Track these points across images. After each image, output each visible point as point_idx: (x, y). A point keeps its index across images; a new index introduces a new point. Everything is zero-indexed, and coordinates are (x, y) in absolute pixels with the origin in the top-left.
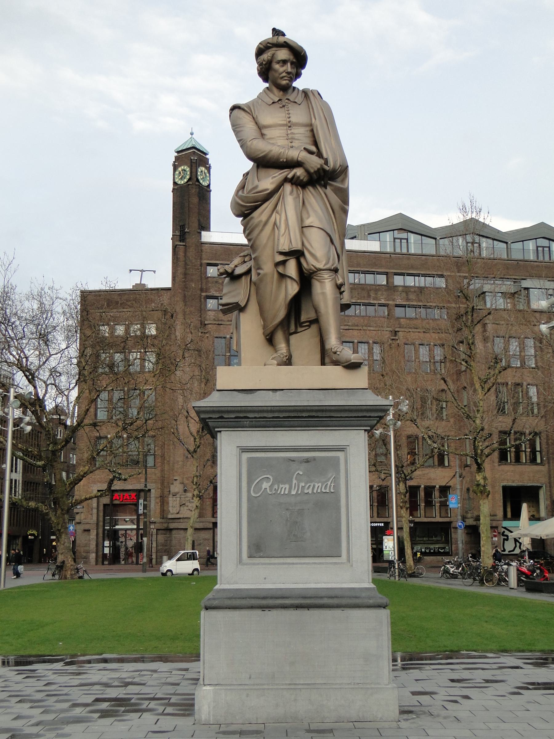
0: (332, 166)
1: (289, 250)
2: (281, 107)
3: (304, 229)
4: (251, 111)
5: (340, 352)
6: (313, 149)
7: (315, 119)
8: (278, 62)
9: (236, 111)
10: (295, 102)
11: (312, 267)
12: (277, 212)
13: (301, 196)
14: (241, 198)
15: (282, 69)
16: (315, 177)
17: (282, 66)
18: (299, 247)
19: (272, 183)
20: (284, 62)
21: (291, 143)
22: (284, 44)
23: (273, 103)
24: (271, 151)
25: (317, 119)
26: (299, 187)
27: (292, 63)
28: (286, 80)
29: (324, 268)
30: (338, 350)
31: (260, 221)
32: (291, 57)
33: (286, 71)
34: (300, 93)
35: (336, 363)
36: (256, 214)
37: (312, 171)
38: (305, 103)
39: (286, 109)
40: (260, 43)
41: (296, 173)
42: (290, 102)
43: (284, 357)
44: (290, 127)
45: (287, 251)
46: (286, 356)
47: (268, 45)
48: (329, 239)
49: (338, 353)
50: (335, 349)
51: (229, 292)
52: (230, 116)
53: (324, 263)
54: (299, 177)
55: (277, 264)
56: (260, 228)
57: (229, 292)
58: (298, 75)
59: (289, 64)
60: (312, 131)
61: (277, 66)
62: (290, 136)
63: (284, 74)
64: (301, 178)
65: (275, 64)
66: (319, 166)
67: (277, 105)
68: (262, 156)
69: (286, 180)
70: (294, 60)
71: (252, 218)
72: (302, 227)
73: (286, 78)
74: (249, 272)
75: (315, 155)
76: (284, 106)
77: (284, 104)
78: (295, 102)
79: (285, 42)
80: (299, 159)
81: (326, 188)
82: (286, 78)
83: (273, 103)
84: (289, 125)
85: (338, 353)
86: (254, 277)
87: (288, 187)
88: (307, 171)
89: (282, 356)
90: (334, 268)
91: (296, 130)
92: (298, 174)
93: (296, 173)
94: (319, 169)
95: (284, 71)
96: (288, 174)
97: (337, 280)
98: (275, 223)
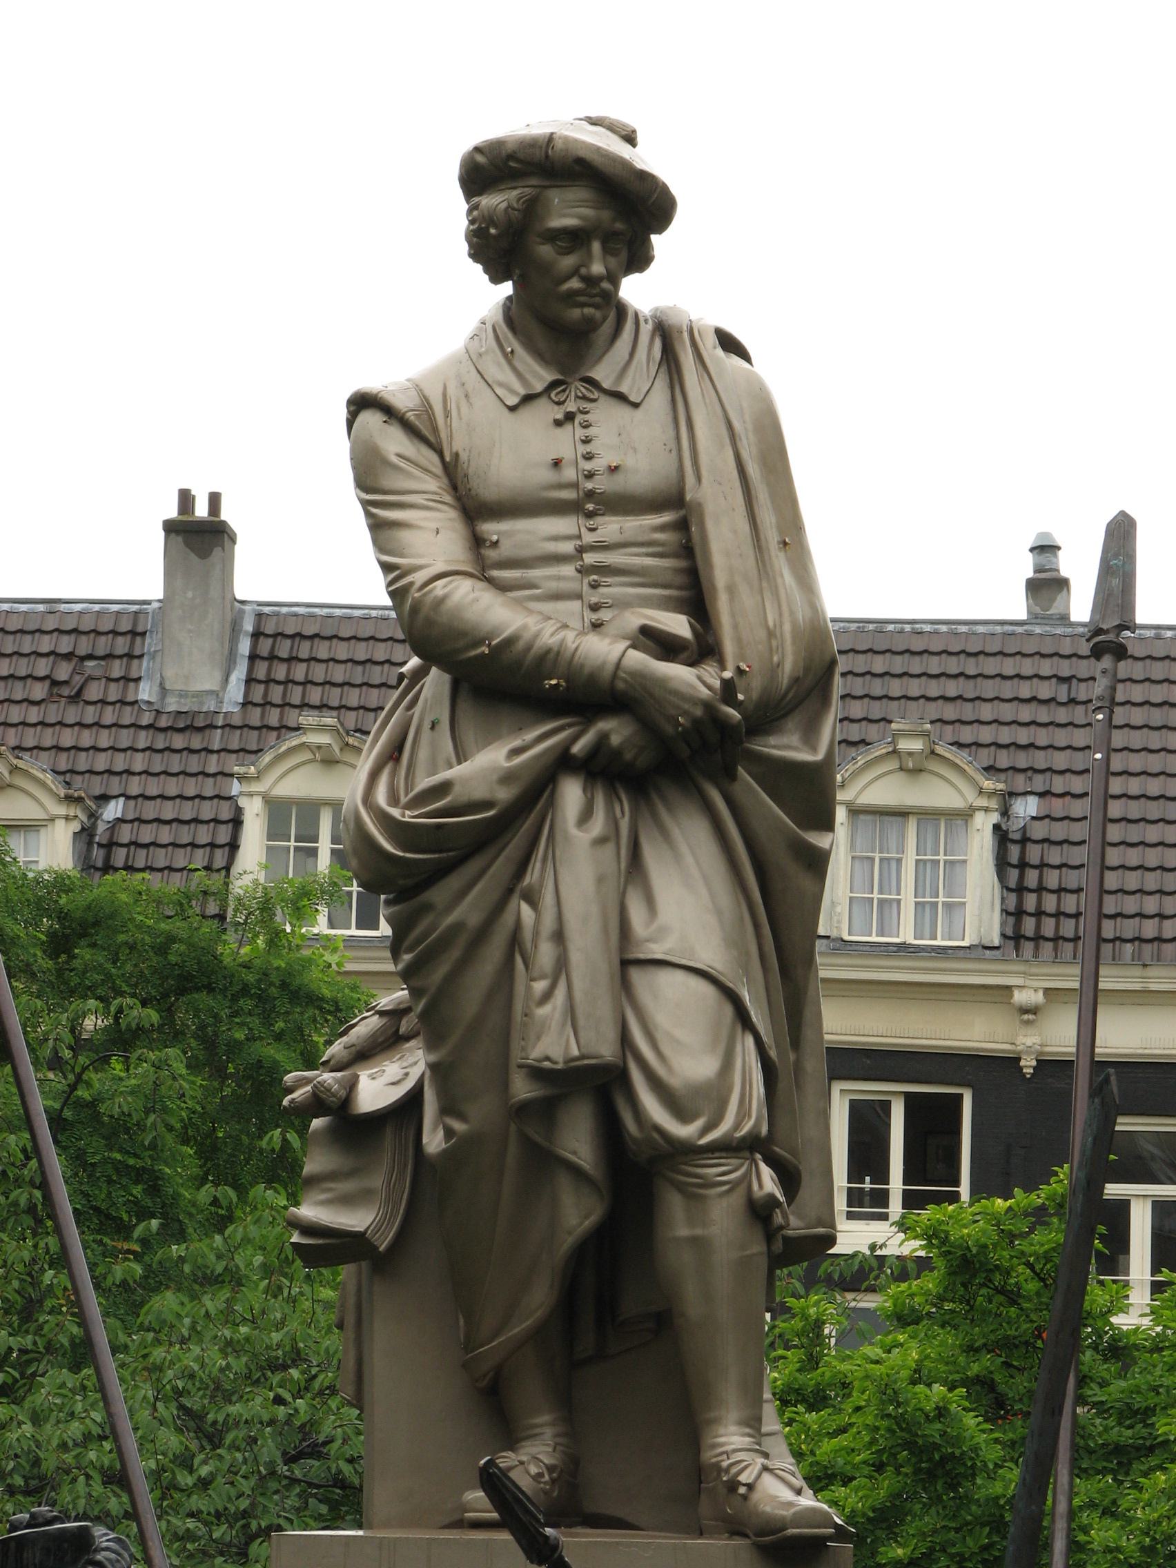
0: (755, 695)
1: (566, 1062)
2: (558, 423)
3: (636, 975)
4: (435, 430)
5: (750, 1487)
6: (679, 625)
7: (699, 478)
8: (554, 236)
9: (370, 419)
10: (620, 397)
11: (656, 1135)
12: (531, 898)
13: (624, 824)
14: (385, 820)
15: (568, 262)
16: (684, 752)
17: (567, 252)
18: (606, 1049)
19: (507, 778)
20: (575, 239)
21: (594, 586)
22: (577, 168)
23: (528, 399)
24: (509, 642)
25: (704, 480)
26: (618, 786)
27: (609, 239)
28: (583, 305)
29: (703, 1142)
30: (743, 1478)
31: (458, 927)
32: (606, 215)
33: (583, 271)
34: (646, 329)
35: (736, 1528)
36: (438, 894)
37: (669, 729)
38: (658, 400)
39: (580, 433)
40: (477, 149)
41: (603, 738)
42: (596, 395)
43: (540, 1475)
44: (590, 515)
45: (559, 1066)
46: (550, 1469)
47: (512, 164)
48: (728, 1010)
49: (742, 1490)
50: (734, 1470)
51: (331, 1176)
52: (350, 424)
53: (699, 1123)
54: (617, 753)
55: (523, 1110)
56: (455, 953)
57: (331, 1176)
58: (639, 259)
59: (596, 246)
60: (682, 526)
61: (545, 251)
62: (590, 558)
63: (575, 284)
64: (628, 756)
65: (538, 240)
66: (698, 712)
67: (546, 411)
68: (470, 659)
69: (563, 763)
70: (619, 226)
71: (427, 908)
72: (626, 964)
73: (582, 299)
74: (411, 1105)
75: (685, 655)
76: (570, 417)
77: (571, 406)
78: (620, 397)
79: (580, 161)
80: (620, 685)
81: (732, 776)
82: (582, 299)
83: (528, 399)
84: (590, 507)
85: (742, 1490)
86: (433, 1141)
87: (571, 793)
88: (647, 725)
89: (533, 1470)
90: (744, 1138)
91: (611, 527)
92: (615, 740)
93: (603, 738)
94: (696, 722)
95: (575, 272)
96: (575, 739)
97: (755, 1187)
98: (515, 941)
